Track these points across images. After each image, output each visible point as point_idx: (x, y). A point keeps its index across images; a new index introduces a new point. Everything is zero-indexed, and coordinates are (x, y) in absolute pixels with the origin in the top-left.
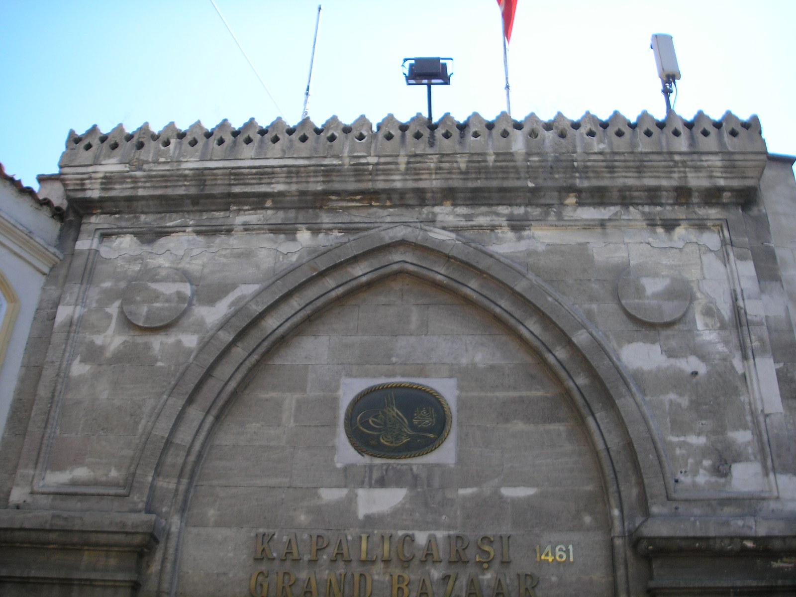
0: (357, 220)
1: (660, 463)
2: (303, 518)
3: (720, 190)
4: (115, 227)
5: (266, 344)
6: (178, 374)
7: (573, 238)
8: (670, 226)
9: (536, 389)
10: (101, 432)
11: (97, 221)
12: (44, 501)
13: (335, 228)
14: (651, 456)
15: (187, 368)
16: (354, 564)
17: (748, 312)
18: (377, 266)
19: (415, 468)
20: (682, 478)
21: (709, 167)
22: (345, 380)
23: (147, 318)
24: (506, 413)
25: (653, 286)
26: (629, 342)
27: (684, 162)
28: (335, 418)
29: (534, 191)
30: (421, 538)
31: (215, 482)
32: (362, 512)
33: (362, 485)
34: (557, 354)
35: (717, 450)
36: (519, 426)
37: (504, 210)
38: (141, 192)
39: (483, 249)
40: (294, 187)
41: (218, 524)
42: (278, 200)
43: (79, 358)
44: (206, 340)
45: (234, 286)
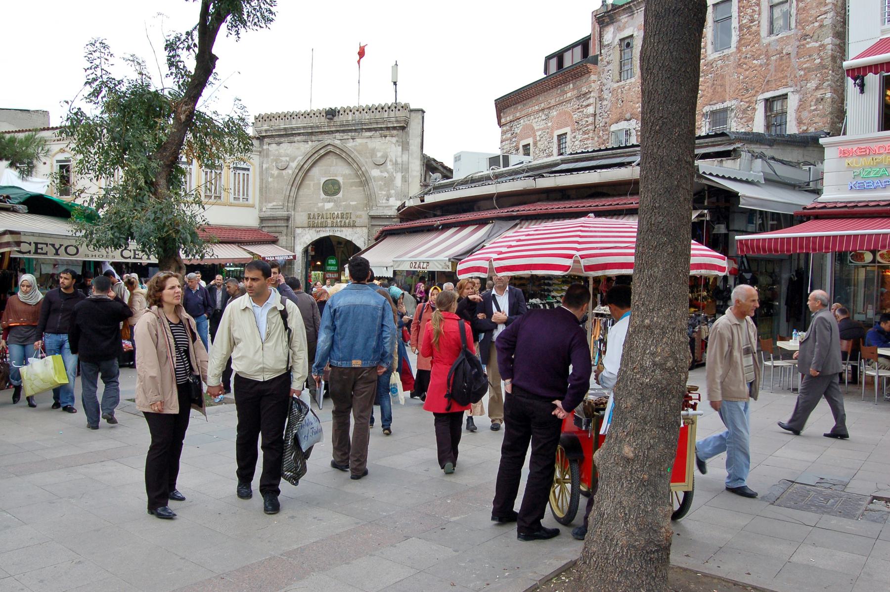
2: (316, 210)
7: (365, 141)
8: (385, 137)
12: (269, 210)
24: (352, 185)
25: (379, 154)
30: (336, 214)
32: (326, 208)
36: (354, 188)
37: (350, 134)
38: (274, 134)
40: (305, 131)
42: (303, 134)
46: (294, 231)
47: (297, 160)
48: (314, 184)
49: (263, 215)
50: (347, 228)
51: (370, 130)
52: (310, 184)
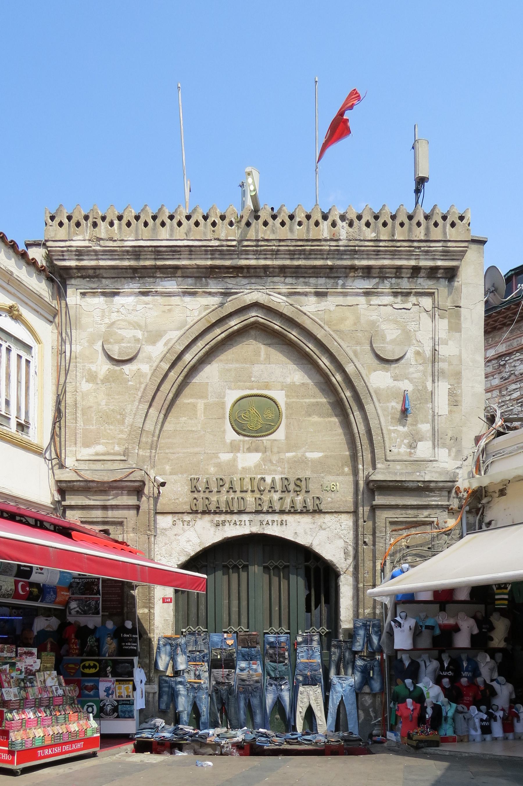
5: (186, 370)
14: (379, 438)
16: (238, 492)
19: (265, 441)
22: (228, 391)
23: (120, 354)
26: (375, 371)
30: (269, 480)
31: (167, 451)
34: (337, 377)
39: (301, 308)
41: (171, 474)
44: (154, 368)
45: (165, 332)
46: (155, 521)
48: (206, 406)
49: (66, 475)
50: (297, 517)
52: (195, 406)
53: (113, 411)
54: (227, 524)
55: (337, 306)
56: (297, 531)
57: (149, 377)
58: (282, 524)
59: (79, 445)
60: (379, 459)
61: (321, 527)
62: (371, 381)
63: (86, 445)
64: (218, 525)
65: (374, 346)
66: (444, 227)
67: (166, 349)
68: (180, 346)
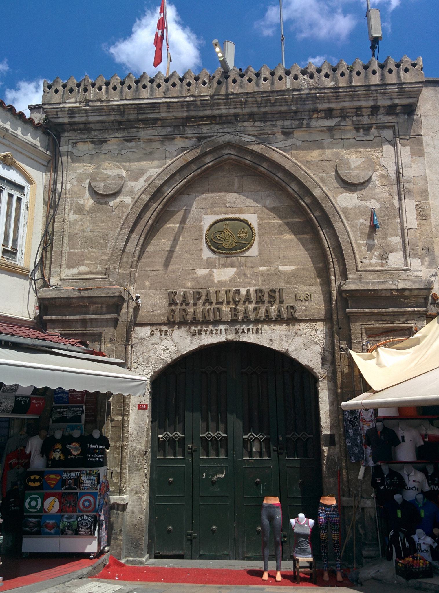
0: (205, 131)
1: (354, 254)
3: (396, 105)
4: (79, 138)
6: (124, 218)
8: (367, 129)
9: (295, 218)
10: (90, 249)
11: (69, 135)
13: (194, 137)
15: (128, 215)
16: (214, 304)
17: (404, 175)
18: (217, 157)
20: (364, 260)
21: (390, 92)
22: (204, 216)
23: (105, 189)
27: (376, 90)
28: (201, 235)
29: (296, 112)
30: (243, 291)
33: (215, 267)
34: (305, 200)
35: (382, 247)
37: (279, 123)
41: (150, 289)
43: (72, 211)
44: (135, 199)
45: (147, 170)
47: (145, 177)
49: (49, 293)
51: (329, 113)
53: (97, 236)
54: (204, 333)
55: (303, 141)
56: (273, 338)
57: (130, 207)
58: (257, 332)
59: (63, 266)
60: (350, 270)
61: (296, 333)
62: (338, 202)
63: (70, 266)
64: (194, 334)
65: (339, 172)
66: (398, 73)
67: (147, 185)
68: (159, 181)
